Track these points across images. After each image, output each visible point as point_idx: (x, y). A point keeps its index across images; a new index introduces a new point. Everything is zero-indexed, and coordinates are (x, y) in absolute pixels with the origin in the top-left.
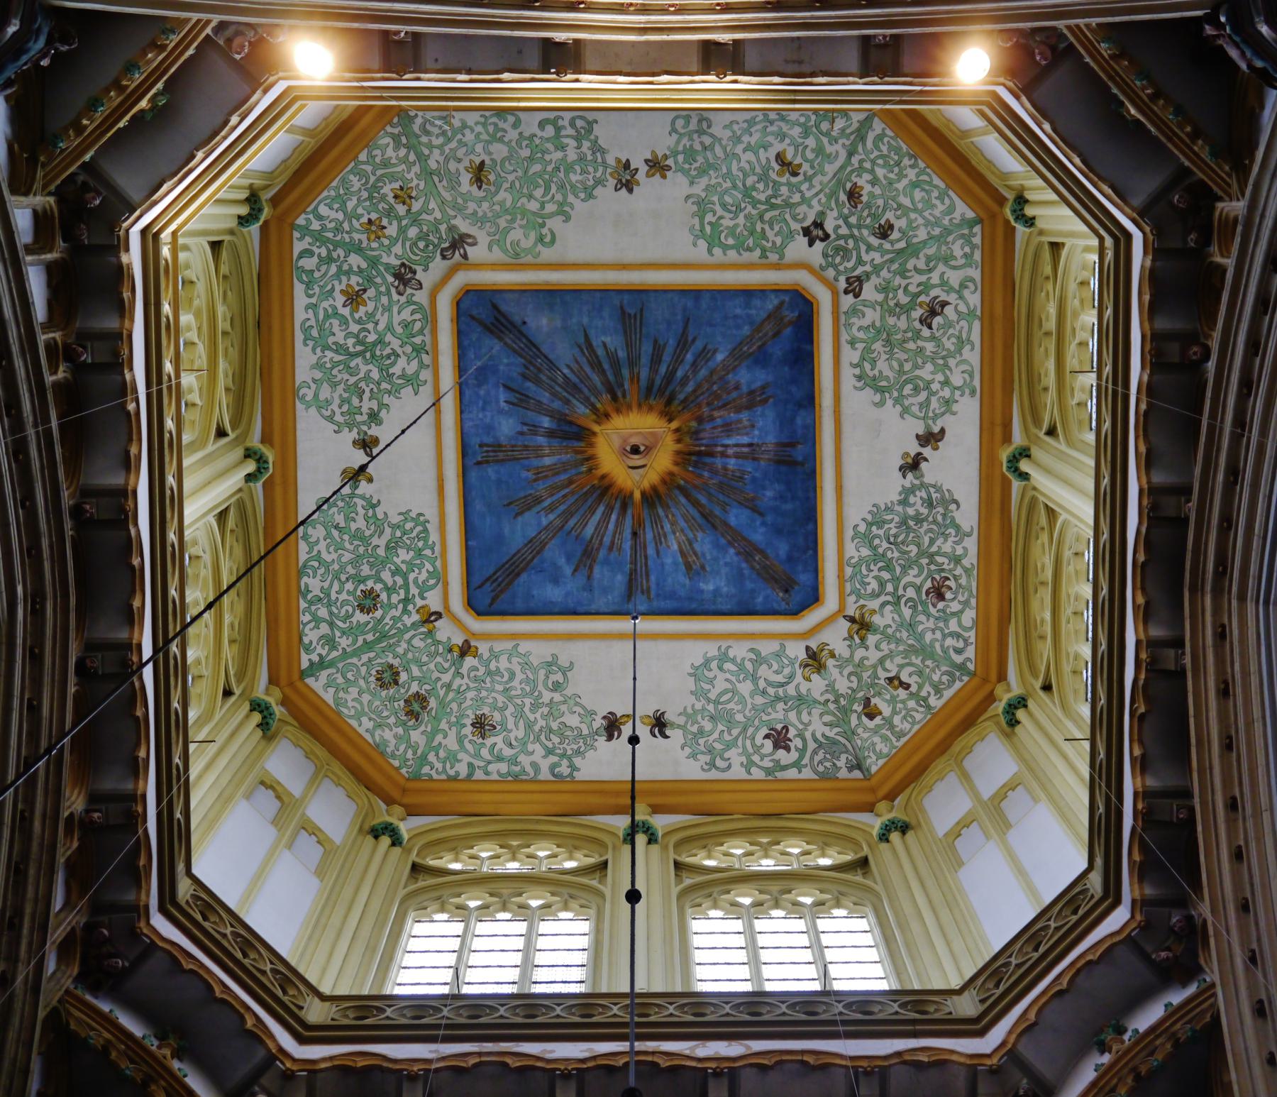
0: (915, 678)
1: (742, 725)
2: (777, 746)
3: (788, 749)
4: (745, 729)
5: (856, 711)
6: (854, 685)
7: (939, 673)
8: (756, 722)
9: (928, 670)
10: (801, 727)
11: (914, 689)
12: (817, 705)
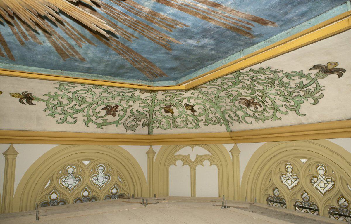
0: (201, 111)
1: (90, 103)
2: (107, 113)
3: (114, 115)
4: (91, 105)
5: (161, 106)
6: (167, 99)
7: (213, 115)
8: (100, 103)
9: (209, 111)
10: (126, 106)
11: (196, 114)
12: (140, 100)
